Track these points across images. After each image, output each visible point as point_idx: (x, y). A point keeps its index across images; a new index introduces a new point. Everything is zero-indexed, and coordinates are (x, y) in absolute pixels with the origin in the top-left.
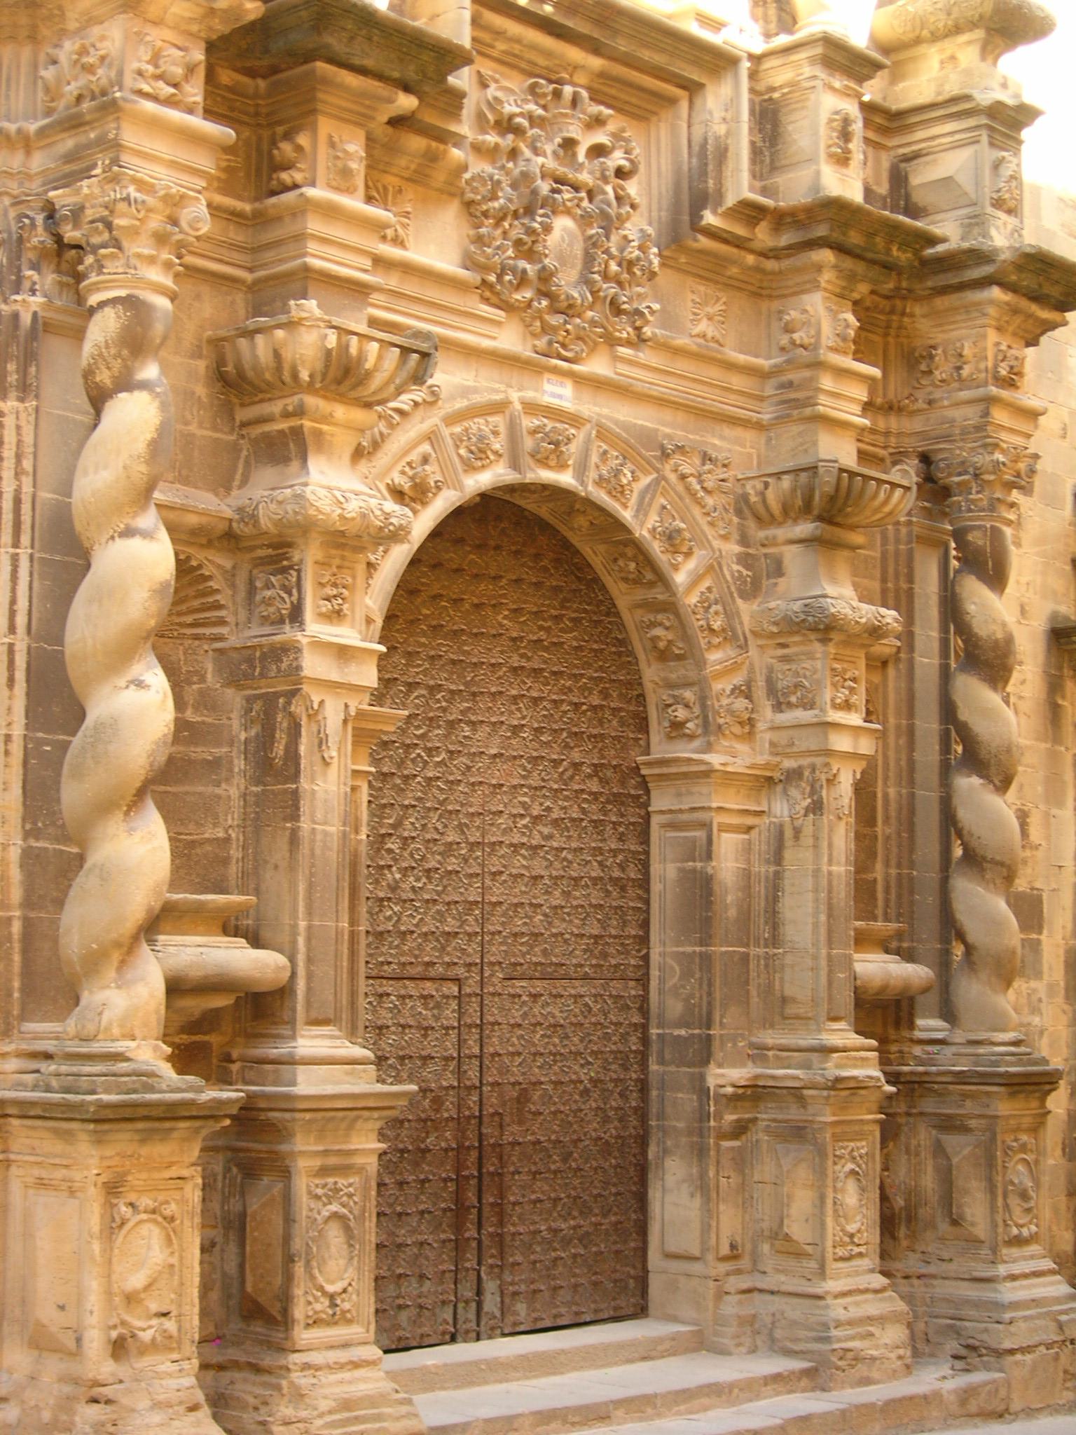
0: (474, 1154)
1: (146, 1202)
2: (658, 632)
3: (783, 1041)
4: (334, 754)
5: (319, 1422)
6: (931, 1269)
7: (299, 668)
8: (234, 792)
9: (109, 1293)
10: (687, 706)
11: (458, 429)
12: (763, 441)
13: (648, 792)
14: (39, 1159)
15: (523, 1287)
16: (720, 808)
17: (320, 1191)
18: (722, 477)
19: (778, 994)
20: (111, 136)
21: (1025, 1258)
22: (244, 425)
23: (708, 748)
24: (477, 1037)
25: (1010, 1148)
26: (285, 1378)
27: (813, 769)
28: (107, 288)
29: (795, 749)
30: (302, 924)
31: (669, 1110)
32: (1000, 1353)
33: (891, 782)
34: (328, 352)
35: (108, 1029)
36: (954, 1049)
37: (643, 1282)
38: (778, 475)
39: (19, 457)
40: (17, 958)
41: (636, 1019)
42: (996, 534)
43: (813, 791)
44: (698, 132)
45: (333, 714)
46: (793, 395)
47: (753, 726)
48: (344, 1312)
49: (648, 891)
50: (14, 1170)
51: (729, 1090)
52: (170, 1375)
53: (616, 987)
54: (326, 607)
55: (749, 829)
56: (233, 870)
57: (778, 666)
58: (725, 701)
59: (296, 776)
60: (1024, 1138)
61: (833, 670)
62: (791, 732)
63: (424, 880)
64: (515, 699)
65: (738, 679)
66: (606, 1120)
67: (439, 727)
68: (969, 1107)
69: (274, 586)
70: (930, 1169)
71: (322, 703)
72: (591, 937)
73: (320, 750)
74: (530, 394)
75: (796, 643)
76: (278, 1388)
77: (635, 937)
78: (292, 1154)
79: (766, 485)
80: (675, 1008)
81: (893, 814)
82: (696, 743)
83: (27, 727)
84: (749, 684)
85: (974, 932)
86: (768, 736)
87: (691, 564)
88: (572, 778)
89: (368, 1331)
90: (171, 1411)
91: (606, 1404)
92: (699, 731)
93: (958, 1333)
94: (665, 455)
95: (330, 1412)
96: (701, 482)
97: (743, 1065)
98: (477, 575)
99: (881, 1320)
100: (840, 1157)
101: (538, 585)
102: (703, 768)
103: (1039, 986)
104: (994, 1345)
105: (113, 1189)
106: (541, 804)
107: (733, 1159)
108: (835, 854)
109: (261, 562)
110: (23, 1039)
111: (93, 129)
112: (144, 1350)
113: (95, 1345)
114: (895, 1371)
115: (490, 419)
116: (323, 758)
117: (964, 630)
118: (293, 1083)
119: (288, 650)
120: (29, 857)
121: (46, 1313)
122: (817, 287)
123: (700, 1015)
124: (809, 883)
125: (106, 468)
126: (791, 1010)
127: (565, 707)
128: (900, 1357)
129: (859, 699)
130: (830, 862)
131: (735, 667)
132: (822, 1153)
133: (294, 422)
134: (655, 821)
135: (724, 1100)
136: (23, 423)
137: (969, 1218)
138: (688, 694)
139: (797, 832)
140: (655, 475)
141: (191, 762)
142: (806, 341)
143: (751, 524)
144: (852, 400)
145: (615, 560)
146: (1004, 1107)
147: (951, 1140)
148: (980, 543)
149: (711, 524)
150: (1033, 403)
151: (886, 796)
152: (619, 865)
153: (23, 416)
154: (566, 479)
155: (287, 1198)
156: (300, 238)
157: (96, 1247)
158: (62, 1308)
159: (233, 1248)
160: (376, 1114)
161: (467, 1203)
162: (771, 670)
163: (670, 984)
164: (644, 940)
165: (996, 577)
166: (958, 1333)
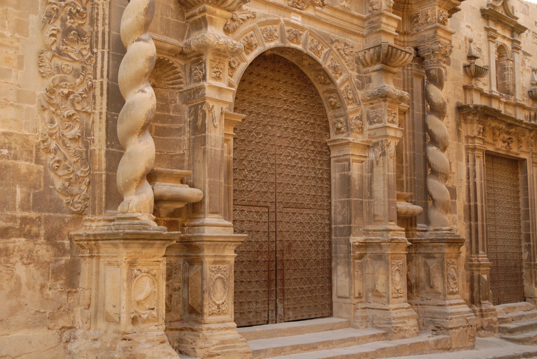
0: (274, 263)
1: (145, 269)
3: (374, 228)
4: (218, 124)
5: (213, 348)
6: (424, 302)
7: (205, 94)
8: (186, 138)
9: (129, 301)
10: (341, 123)
11: (263, 28)
12: (364, 41)
13: (330, 151)
14: (108, 255)
15: (291, 306)
16: (352, 155)
17: (213, 269)
18: (351, 51)
19: (372, 213)
21: (455, 299)
22: (188, 18)
23: (348, 135)
24: (275, 225)
25: (449, 263)
26: (201, 333)
27: (382, 141)
29: (376, 136)
30: (207, 180)
31: (338, 251)
32: (448, 329)
33: (408, 149)
35: (131, 209)
36: (429, 232)
37: (331, 305)
38: (369, 49)
39: (104, 19)
40: (104, 187)
41: (327, 222)
42: (440, 71)
43: (382, 149)
45: (217, 111)
46: (373, 25)
47: (363, 130)
48: (223, 311)
49: (330, 182)
50: (101, 259)
51: (357, 244)
52: (154, 331)
53: (320, 212)
54: (214, 75)
55: (362, 162)
56: (186, 164)
57: (370, 111)
58: (353, 121)
59: (205, 132)
60: (453, 260)
61: (388, 110)
63: (256, 174)
64: (286, 119)
65: (358, 114)
66: (318, 254)
67: (260, 126)
69: (197, 69)
70: (423, 270)
71: (213, 106)
72: (312, 195)
73: (213, 122)
74: (287, 19)
75: (376, 103)
76: (199, 336)
77: (326, 196)
78: (203, 256)
79: (365, 53)
80: (340, 218)
81: (408, 160)
82: (345, 135)
83: (108, 109)
84: (361, 116)
85: (435, 195)
86: (367, 132)
87: (342, 78)
88: (305, 145)
89: (231, 317)
90: (154, 343)
91: (316, 343)
92: (346, 131)
93: (434, 323)
94: (332, 42)
95: (217, 345)
96: (344, 52)
97: (362, 236)
98: (272, 79)
99: (408, 318)
100: (394, 265)
101: (292, 84)
102: (347, 141)
103: (456, 216)
104: (446, 326)
105: (132, 264)
106: (295, 153)
107: (359, 266)
108: (390, 169)
109: (193, 62)
110: (106, 215)
112: (144, 322)
113: (125, 319)
114: (413, 334)
115: (273, 26)
116: (214, 125)
117: (430, 101)
118: (204, 232)
119: (201, 89)
120: (107, 153)
121: (109, 308)
123: (348, 220)
124: (382, 178)
125: (130, 17)
126: (376, 219)
127: (302, 123)
128: (415, 330)
129: (397, 120)
130: (388, 171)
131: (356, 111)
132: (387, 263)
134: (332, 160)
135: (356, 247)
136: (105, 8)
137: (436, 285)
138: (342, 119)
139: (377, 163)
140: (329, 48)
141: (172, 129)
142: (377, 8)
143: (361, 67)
144: (392, 27)
145: (317, 77)
146: (446, 250)
147: (430, 261)
148: (434, 73)
149: (348, 65)
150: (450, 29)
151: (406, 154)
152: (321, 173)
153: (105, 5)
154: (300, 47)
155: (202, 271)
157: (125, 284)
158: (114, 306)
159: (186, 289)
160: (233, 244)
161: (272, 279)
162: (368, 112)
163: (338, 211)
164: (329, 197)
165: (440, 85)
166: (434, 323)
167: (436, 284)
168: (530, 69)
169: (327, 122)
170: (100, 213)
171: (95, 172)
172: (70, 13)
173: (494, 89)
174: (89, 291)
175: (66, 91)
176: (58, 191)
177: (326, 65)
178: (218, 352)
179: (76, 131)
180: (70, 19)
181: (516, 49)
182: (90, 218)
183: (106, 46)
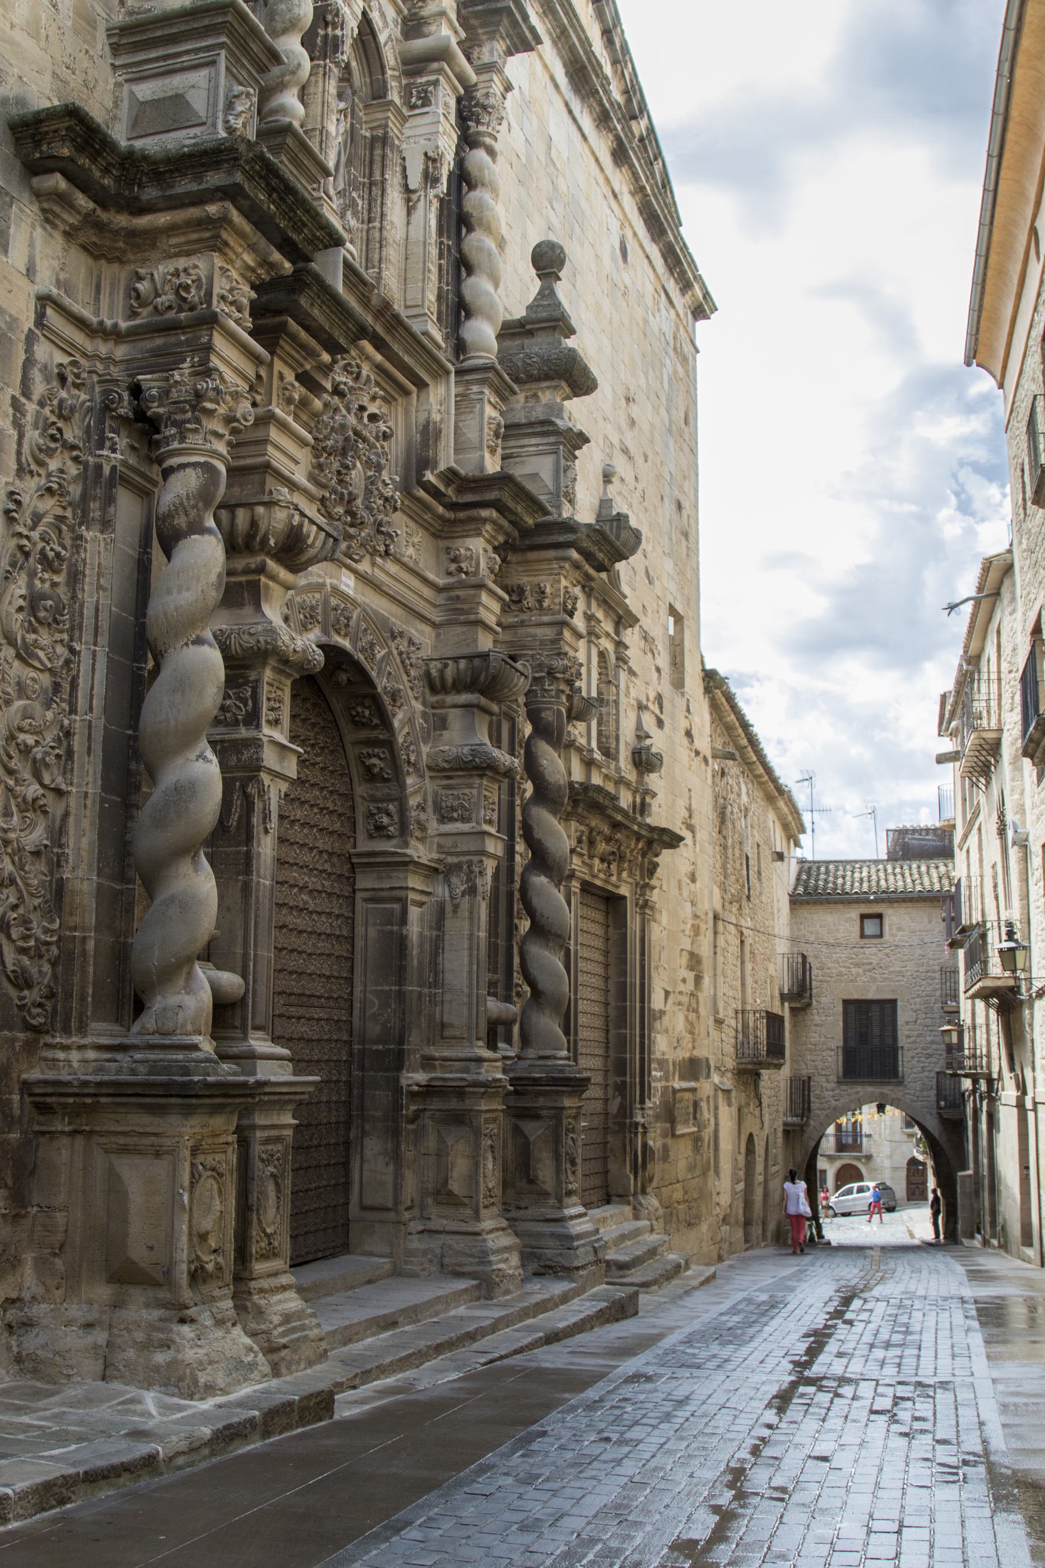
2: (375, 761)
7: (259, 759)
10: (389, 815)
16: (413, 889)
19: (438, 1021)
20: (205, 339)
28: (180, 455)
34: (293, 526)
35: (183, 1026)
36: (529, 1062)
38: (456, 659)
41: (345, 1038)
43: (469, 880)
44: (422, 417)
51: (416, 1088)
54: (272, 716)
55: (423, 904)
62: (455, 838)
68: (541, 1101)
73: (264, 823)
79: (446, 666)
80: (374, 1029)
82: (394, 842)
83: (105, 788)
95: (280, 1325)
99: (507, 1249)
104: (567, 1265)
111: (184, 333)
118: (253, 1073)
121: (138, 1253)
122: (479, 535)
125: (188, 590)
126: (447, 1033)
132: (477, 1133)
133: (251, 577)
134: (359, 896)
138: (391, 807)
139: (456, 908)
142: (471, 569)
143: (427, 691)
149: (412, 689)
156: (266, 441)
158: (151, 1248)
162: (436, 794)
166: (539, 1257)
167: (540, 1174)
168: (635, 703)
169: (353, 808)
170: (82, 1030)
171: (68, 933)
172: (44, 558)
173: (594, 745)
174: (64, 1214)
175: (30, 740)
176: (8, 977)
177: (382, 684)
178: (284, 1341)
179: (37, 836)
180: (43, 570)
181: (621, 659)
182: (58, 1040)
183: (103, 640)
